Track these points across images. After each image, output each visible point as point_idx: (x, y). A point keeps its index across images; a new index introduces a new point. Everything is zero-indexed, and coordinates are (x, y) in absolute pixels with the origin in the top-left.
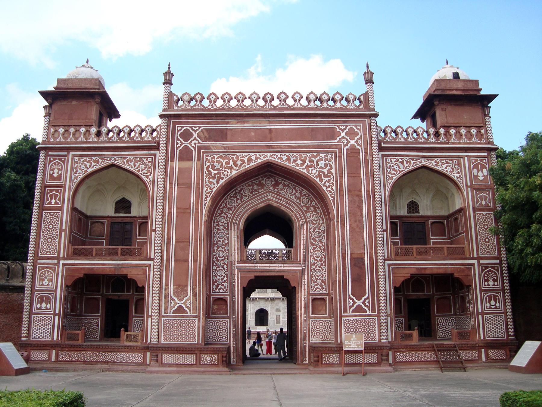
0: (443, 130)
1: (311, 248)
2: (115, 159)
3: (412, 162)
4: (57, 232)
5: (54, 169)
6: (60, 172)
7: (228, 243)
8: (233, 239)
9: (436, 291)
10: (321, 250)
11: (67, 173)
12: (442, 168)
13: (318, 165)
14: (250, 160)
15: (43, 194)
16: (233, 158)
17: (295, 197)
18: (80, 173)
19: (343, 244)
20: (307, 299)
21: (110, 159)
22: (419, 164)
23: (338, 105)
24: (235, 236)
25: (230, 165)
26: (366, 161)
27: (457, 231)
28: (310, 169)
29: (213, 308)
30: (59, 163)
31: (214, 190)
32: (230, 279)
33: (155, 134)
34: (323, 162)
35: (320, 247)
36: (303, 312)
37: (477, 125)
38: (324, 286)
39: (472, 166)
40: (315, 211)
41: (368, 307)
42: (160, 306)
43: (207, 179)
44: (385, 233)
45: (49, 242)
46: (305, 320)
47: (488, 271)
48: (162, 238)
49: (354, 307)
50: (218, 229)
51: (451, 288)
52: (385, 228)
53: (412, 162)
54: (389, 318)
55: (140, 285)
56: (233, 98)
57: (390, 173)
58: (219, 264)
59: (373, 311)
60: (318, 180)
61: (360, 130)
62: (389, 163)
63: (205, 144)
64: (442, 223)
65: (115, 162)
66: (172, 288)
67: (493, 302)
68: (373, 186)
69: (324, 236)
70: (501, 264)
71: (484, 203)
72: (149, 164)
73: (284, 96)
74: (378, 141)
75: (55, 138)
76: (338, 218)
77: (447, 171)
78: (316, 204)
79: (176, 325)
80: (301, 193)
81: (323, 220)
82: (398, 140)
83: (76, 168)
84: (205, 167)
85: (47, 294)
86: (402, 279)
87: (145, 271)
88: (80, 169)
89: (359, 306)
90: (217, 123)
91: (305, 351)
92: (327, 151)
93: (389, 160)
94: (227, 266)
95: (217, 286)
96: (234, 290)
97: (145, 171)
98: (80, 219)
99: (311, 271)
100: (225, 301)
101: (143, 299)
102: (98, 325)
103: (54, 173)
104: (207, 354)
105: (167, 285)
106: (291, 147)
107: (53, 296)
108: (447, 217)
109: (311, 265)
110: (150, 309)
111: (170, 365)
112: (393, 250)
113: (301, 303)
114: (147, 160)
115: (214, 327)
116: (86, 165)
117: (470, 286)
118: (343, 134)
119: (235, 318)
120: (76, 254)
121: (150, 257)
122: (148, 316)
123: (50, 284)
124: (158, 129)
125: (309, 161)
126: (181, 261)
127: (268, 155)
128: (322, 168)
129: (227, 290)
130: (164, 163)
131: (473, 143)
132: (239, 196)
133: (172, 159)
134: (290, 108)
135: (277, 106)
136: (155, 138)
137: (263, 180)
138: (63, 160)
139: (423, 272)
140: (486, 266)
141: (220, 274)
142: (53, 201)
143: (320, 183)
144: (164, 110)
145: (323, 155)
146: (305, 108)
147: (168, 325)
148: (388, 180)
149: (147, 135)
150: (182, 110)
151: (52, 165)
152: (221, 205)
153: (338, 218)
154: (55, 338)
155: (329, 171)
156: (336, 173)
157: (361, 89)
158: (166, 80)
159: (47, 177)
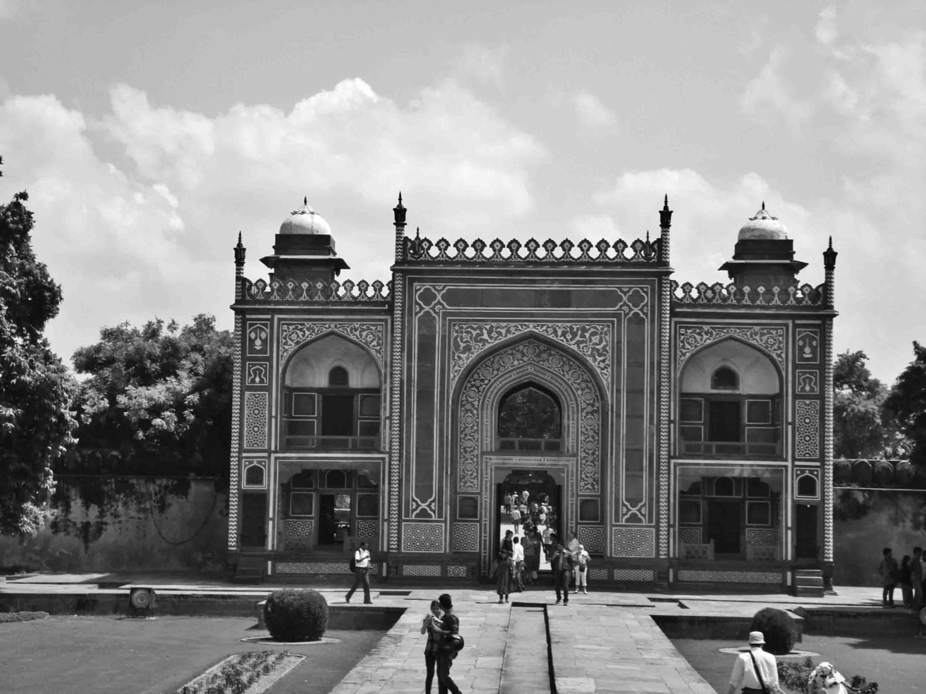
1: (581, 438)
7: (477, 430)
9: (749, 495)
13: (591, 340)
14: (508, 331)
22: (723, 335)
28: (581, 346)
34: (598, 337)
38: (596, 487)
39: (797, 338)
44: (672, 425)
53: (714, 333)
58: (468, 456)
59: (650, 521)
60: (590, 359)
61: (646, 293)
65: (336, 330)
89: (634, 515)
93: (683, 331)
94: (477, 457)
95: (465, 483)
97: (375, 343)
100: (475, 500)
121: (384, 448)
122: (384, 520)
125: (583, 336)
127: (531, 325)
141: (467, 467)
142: (257, 379)
144: (397, 263)
155: (604, 349)
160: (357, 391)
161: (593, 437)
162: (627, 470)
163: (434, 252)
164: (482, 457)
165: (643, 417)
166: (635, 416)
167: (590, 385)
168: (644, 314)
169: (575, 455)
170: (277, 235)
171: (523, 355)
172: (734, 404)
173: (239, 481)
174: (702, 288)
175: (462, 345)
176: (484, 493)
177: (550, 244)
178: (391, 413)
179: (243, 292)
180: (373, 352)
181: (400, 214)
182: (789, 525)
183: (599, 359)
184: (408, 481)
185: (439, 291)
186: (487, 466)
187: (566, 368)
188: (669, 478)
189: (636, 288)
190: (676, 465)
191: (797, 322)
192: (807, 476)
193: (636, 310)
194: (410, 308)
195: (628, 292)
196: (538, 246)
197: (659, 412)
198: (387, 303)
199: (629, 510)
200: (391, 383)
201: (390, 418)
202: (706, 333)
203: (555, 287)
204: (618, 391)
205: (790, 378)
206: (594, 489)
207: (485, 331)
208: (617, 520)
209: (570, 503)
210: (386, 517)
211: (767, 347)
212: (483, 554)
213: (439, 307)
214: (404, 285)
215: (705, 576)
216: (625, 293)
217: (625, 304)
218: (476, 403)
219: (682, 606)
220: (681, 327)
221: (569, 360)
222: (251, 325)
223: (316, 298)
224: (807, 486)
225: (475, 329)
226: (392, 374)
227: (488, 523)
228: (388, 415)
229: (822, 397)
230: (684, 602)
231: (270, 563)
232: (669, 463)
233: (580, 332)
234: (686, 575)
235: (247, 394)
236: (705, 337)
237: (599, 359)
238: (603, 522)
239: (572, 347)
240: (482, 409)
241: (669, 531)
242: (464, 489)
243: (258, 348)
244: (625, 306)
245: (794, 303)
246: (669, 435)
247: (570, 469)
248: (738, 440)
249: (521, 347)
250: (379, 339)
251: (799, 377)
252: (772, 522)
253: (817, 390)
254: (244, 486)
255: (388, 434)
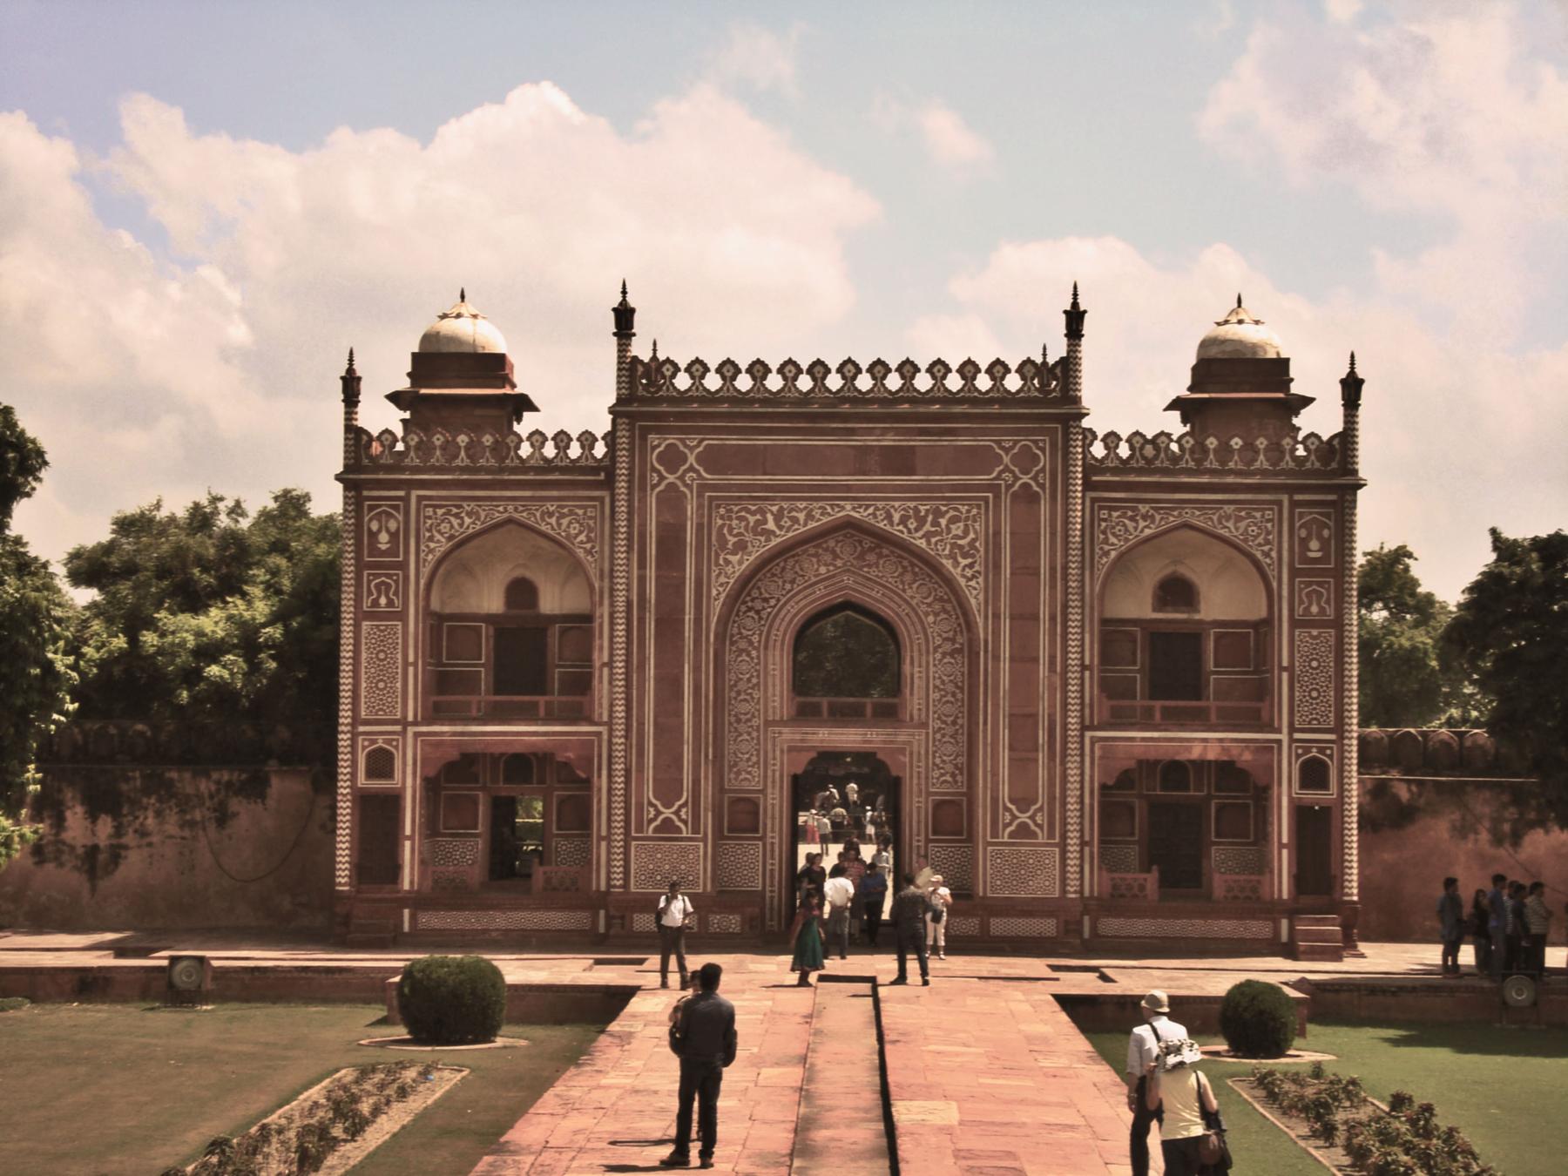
9: (1218, 789)
13: (949, 530)
14: (809, 517)
22: (1173, 520)
34: (961, 525)
38: (959, 778)
44: (1087, 673)
53: (1158, 517)
58: (742, 727)
59: (1051, 835)
60: (948, 563)
61: (1043, 450)
65: (516, 515)
89: (1023, 826)
93: (1104, 514)
95: (738, 773)
97: (582, 537)
100: (754, 804)
117: (1267, 789)
121: (601, 715)
122: (600, 838)
125: (935, 523)
128: (957, 537)
142: (383, 601)
144: (620, 400)
155: (972, 544)
160: (553, 619)
161: (954, 695)
162: (1011, 748)
163: (683, 382)
164: (766, 731)
165: (1036, 660)
166: (1024, 658)
167: (948, 607)
168: (1039, 485)
169: (924, 725)
170: (414, 354)
171: (836, 557)
172: (1191, 638)
173: (354, 775)
174: (1137, 441)
175: (732, 540)
176: (769, 790)
177: (879, 367)
178: (611, 655)
179: (357, 452)
180: (581, 553)
181: (624, 317)
182: (1285, 840)
183: (964, 562)
184: (641, 769)
185: (691, 449)
186: (774, 745)
187: (908, 577)
188: (1082, 762)
189: (1025, 441)
190: (1093, 741)
191: (1298, 497)
192: (1314, 759)
193: (1025, 479)
194: (643, 477)
195: (1012, 448)
196: (859, 371)
197: (1065, 652)
198: (604, 469)
199: (1014, 817)
200: (612, 605)
201: (610, 664)
202: (1144, 518)
203: (889, 441)
204: (996, 616)
205: (1285, 593)
207: (770, 517)
208: (995, 834)
209: (916, 807)
210: (604, 833)
211: (1246, 540)
212: (768, 894)
213: (692, 476)
214: (632, 437)
215: (1143, 927)
216: (1007, 450)
217: (1007, 469)
218: (755, 639)
219: (1105, 978)
220: (1101, 508)
221: (913, 565)
222: (371, 508)
223: (482, 462)
224: (1314, 774)
225: (753, 513)
226: (612, 590)
227: (776, 841)
228: (606, 659)
229: (1339, 624)
230: (1108, 972)
231: (406, 912)
232: (1082, 736)
233: (930, 518)
234: (1112, 926)
235: (365, 624)
236: (1142, 524)
237: (964, 562)
238: (971, 838)
239: (918, 542)
240: (766, 648)
241: (1082, 851)
242: (736, 785)
243: (383, 547)
244: (1006, 473)
245: (1292, 465)
246: (1082, 688)
247: (915, 749)
248: (1199, 699)
249: (832, 543)
250: (591, 530)
251: (1301, 590)
253: (1331, 612)
254: (362, 781)
255: (606, 690)
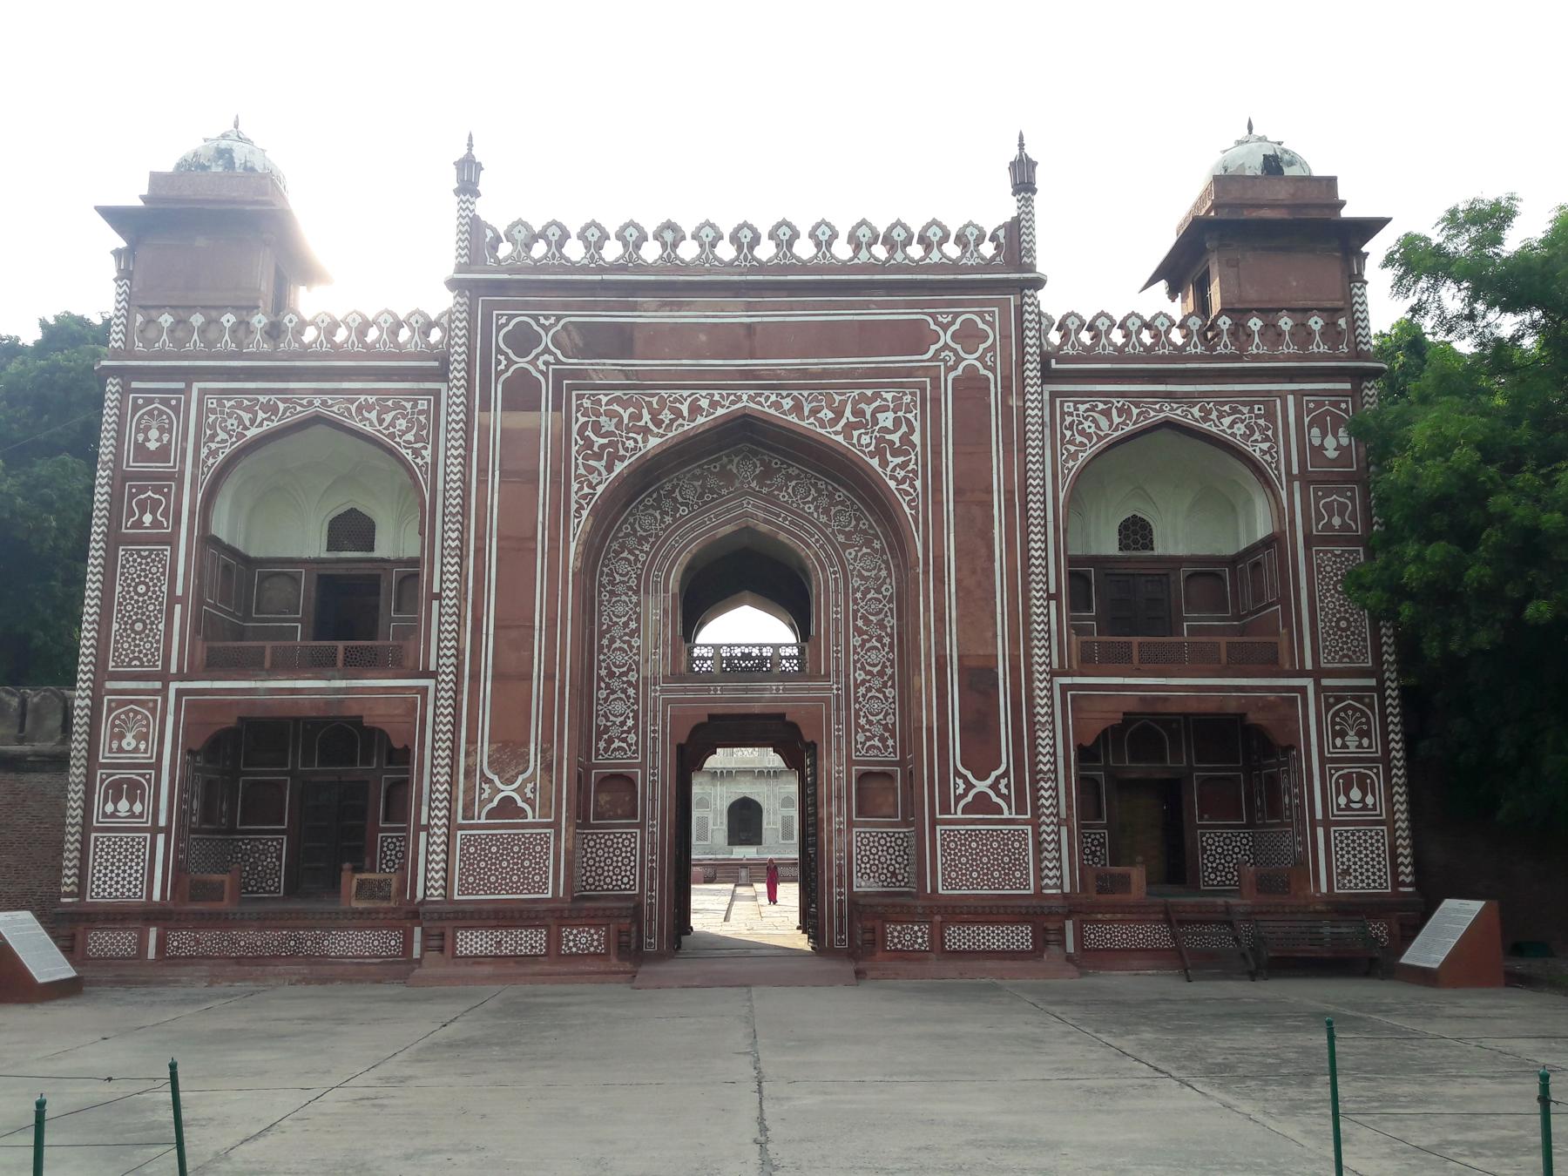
0: (1229, 322)
1: (855, 641)
2: (324, 403)
3: (1135, 411)
4: (161, 604)
5: (148, 428)
6: (166, 437)
7: (638, 629)
8: (652, 618)
9: (1198, 761)
10: (883, 645)
11: (185, 438)
12: (1224, 426)
13: (875, 422)
14: (695, 409)
15: (115, 500)
16: (649, 404)
17: (817, 508)
18: (223, 441)
19: (943, 635)
20: (844, 775)
21: (311, 403)
22: (1154, 417)
23: (935, 256)
24: (658, 610)
25: (642, 423)
26: (1007, 409)
27: (1259, 597)
28: (856, 433)
29: (596, 801)
30: (161, 413)
31: (600, 489)
32: (645, 723)
33: (435, 335)
34: (891, 415)
35: (880, 639)
36: (834, 809)
37: (1328, 305)
38: (890, 742)
39: (1307, 420)
40: (868, 544)
41: (1006, 798)
42: (451, 800)
43: (580, 461)
44: (1053, 603)
45: (137, 633)
46: (840, 830)
47: (1344, 709)
48: (459, 616)
49: (969, 798)
50: (612, 593)
51: (1241, 756)
52: (1053, 590)
53: (1135, 411)
54: (1064, 830)
55: (397, 744)
56: (650, 237)
57: (1069, 442)
59: (1021, 809)
60: (875, 462)
61: (991, 325)
62: (1071, 414)
63: (573, 363)
64: (1218, 577)
66: (485, 748)
67: (1356, 794)
68: (1024, 479)
69: (891, 610)
70: (1380, 689)
71: (1336, 521)
72: (422, 418)
73: (789, 233)
74: (1040, 355)
75: (149, 343)
76: (926, 563)
77: (1234, 435)
78: (871, 526)
79: (494, 849)
80: (831, 496)
81: (888, 569)
82: (1099, 350)
83: (212, 427)
84: (575, 428)
85: (132, 775)
86: (1099, 727)
87: (411, 706)
88: (224, 429)
89: (981, 796)
90: (609, 307)
91: (841, 916)
92: (901, 385)
93: (1069, 407)
94: (636, 688)
95: (610, 741)
96: (654, 753)
97: (410, 437)
98: (227, 567)
99: (856, 700)
100: (629, 781)
101: (406, 783)
102: (279, 858)
103: (147, 439)
104: (577, 926)
105: (471, 740)
106: (804, 374)
107: (149, 781)
108: (1233, 561)
109: (857, 686)
110: (425, 809)
111: (476, 959)
112: (1074, 646)
113: (830, 785)
114: (415, 406)
115: (600, 852)
116: (239, 418)
117: (1291, 747)
118: (945, 338)
119: (657, 824)
120: (215, 665)
122: (419, 828)
123: (142, 746)
124: (445, 320)
125: (854, 413)
126: (511, 677)
128: (885, 430)
129: (636, 751)
130: (462, 416)
131: (1312, 357)
132: (667, 504)
133: (485, 406)
134: (804, 267)
135: (770, 260)
136: (435, 346)
137: (731, 461)
138: (173, 402)
139: (1160, 708)
140: (1339, 694)
141: (616, 710)
142: (148, 519)
143: (880, 470)
144: (460, 268)
145: (889, 396)
146: (844, 267)
147: (472, 850)
148: (1066, 461)
149: (412, 337)
150: (510, 271)
151: (141, 417)
152: (620, 529)
153: (926, 563)
154: (157, 896)
155: (905, 439)
156: (924, 445)
157: (998, 209)
158: (460, 180)
159: (129, 449)
174: (1102, 324)
195: (952, 323)
196: (756, 240)
206: (886, 747)
232: (1051, 681)
252: (1250, 815)
